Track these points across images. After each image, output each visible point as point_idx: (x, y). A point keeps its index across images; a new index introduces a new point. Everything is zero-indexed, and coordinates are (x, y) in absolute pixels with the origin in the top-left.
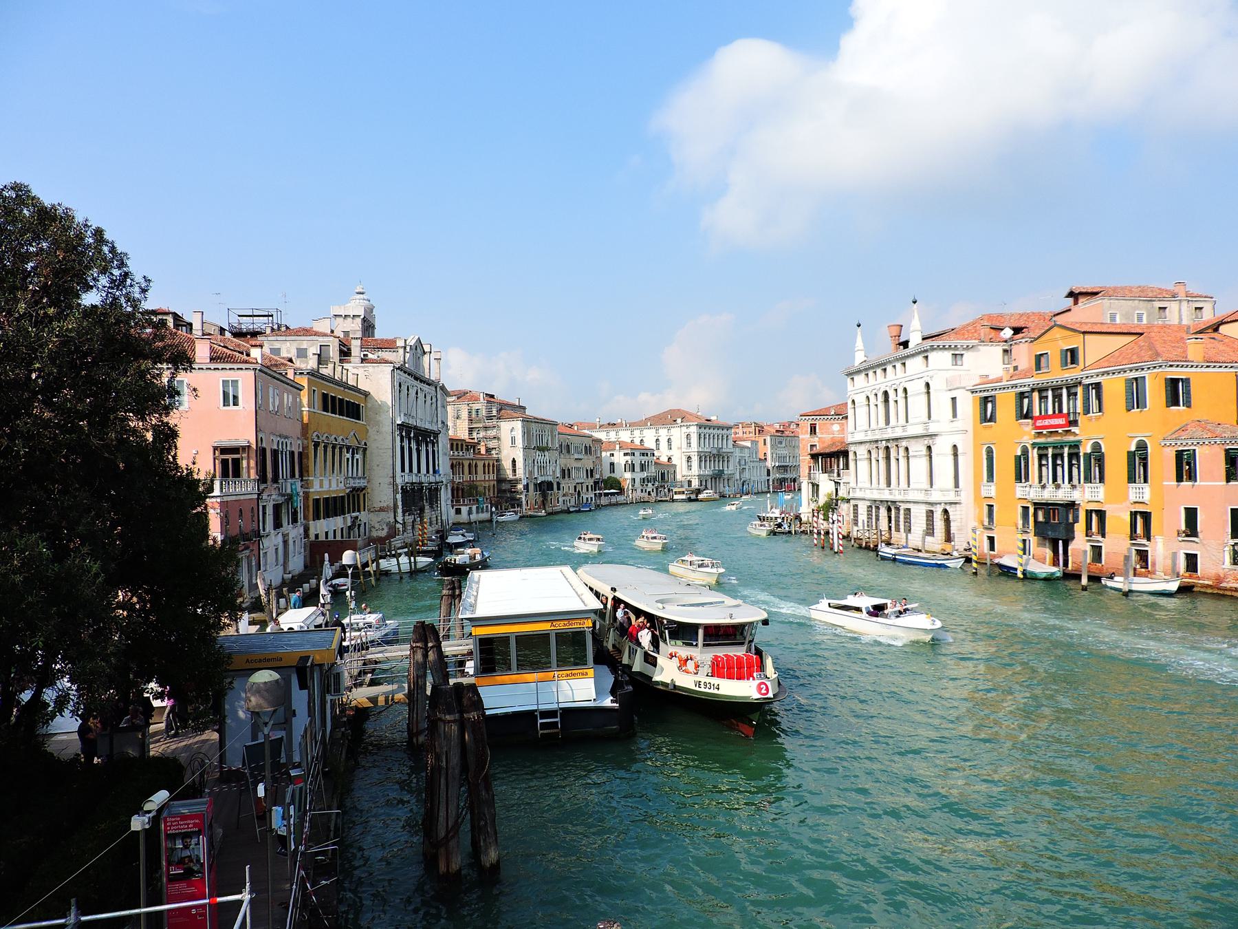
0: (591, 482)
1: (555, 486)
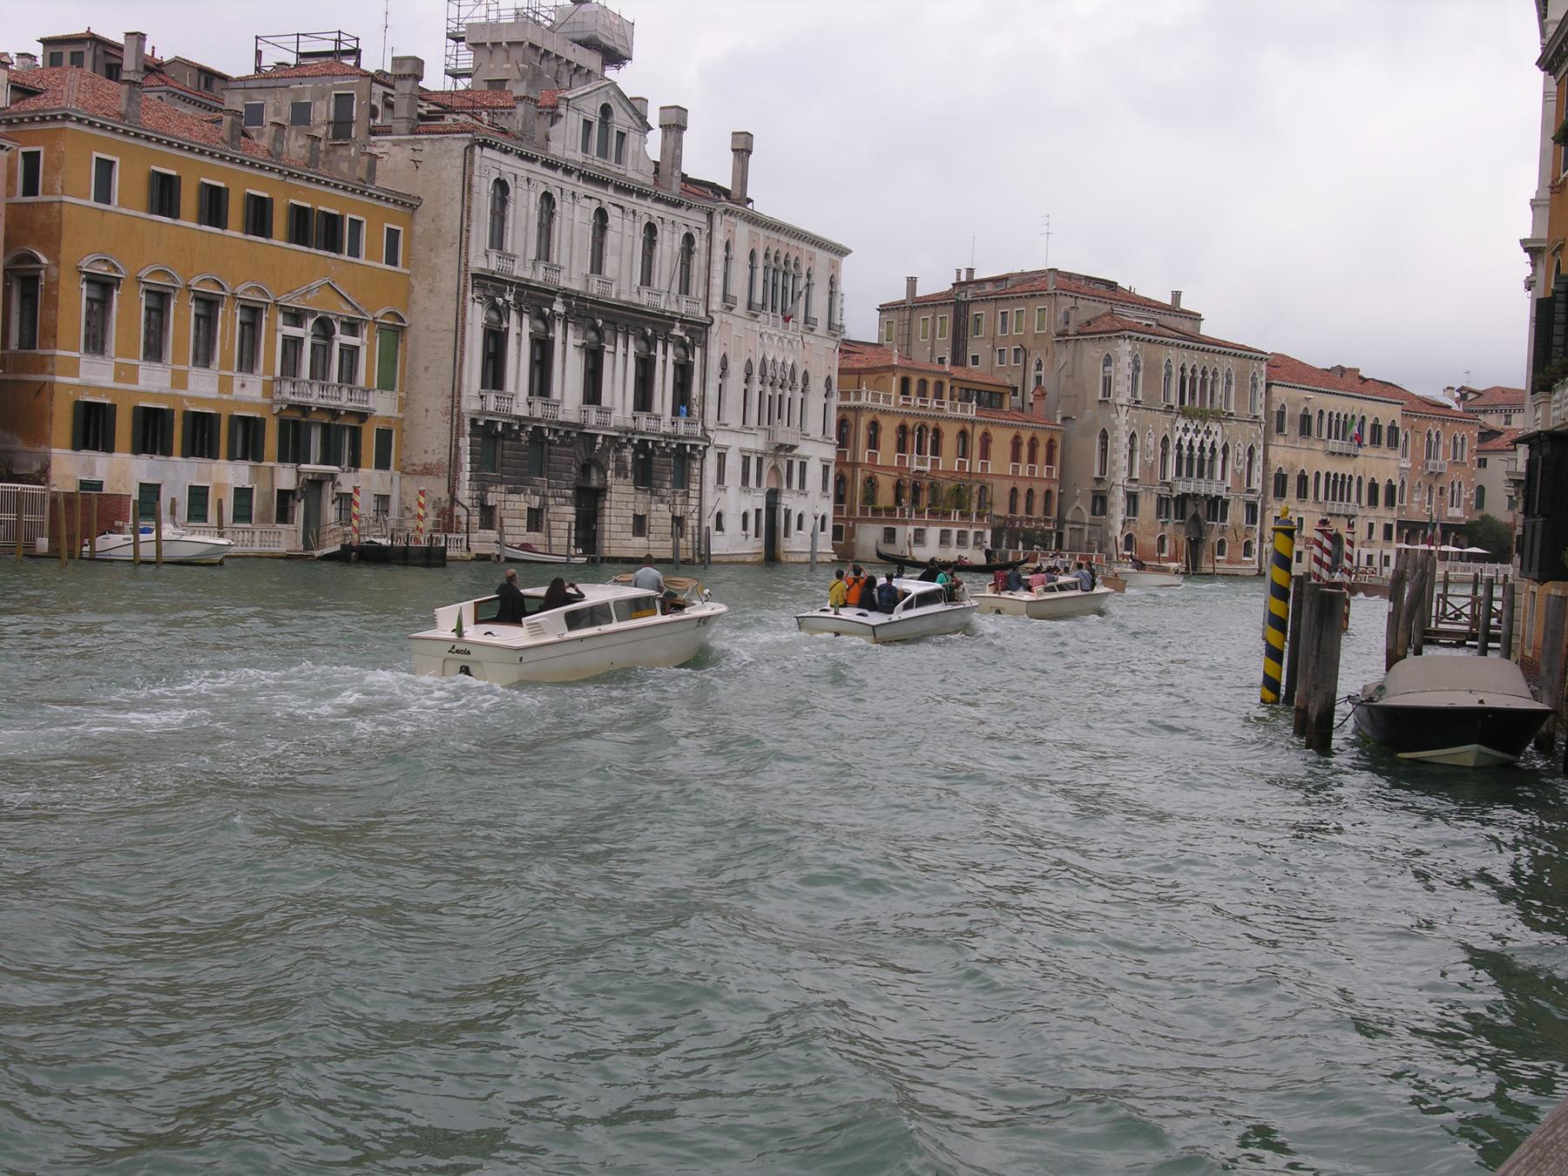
0: (1384, 515)
1: (1236, 513)
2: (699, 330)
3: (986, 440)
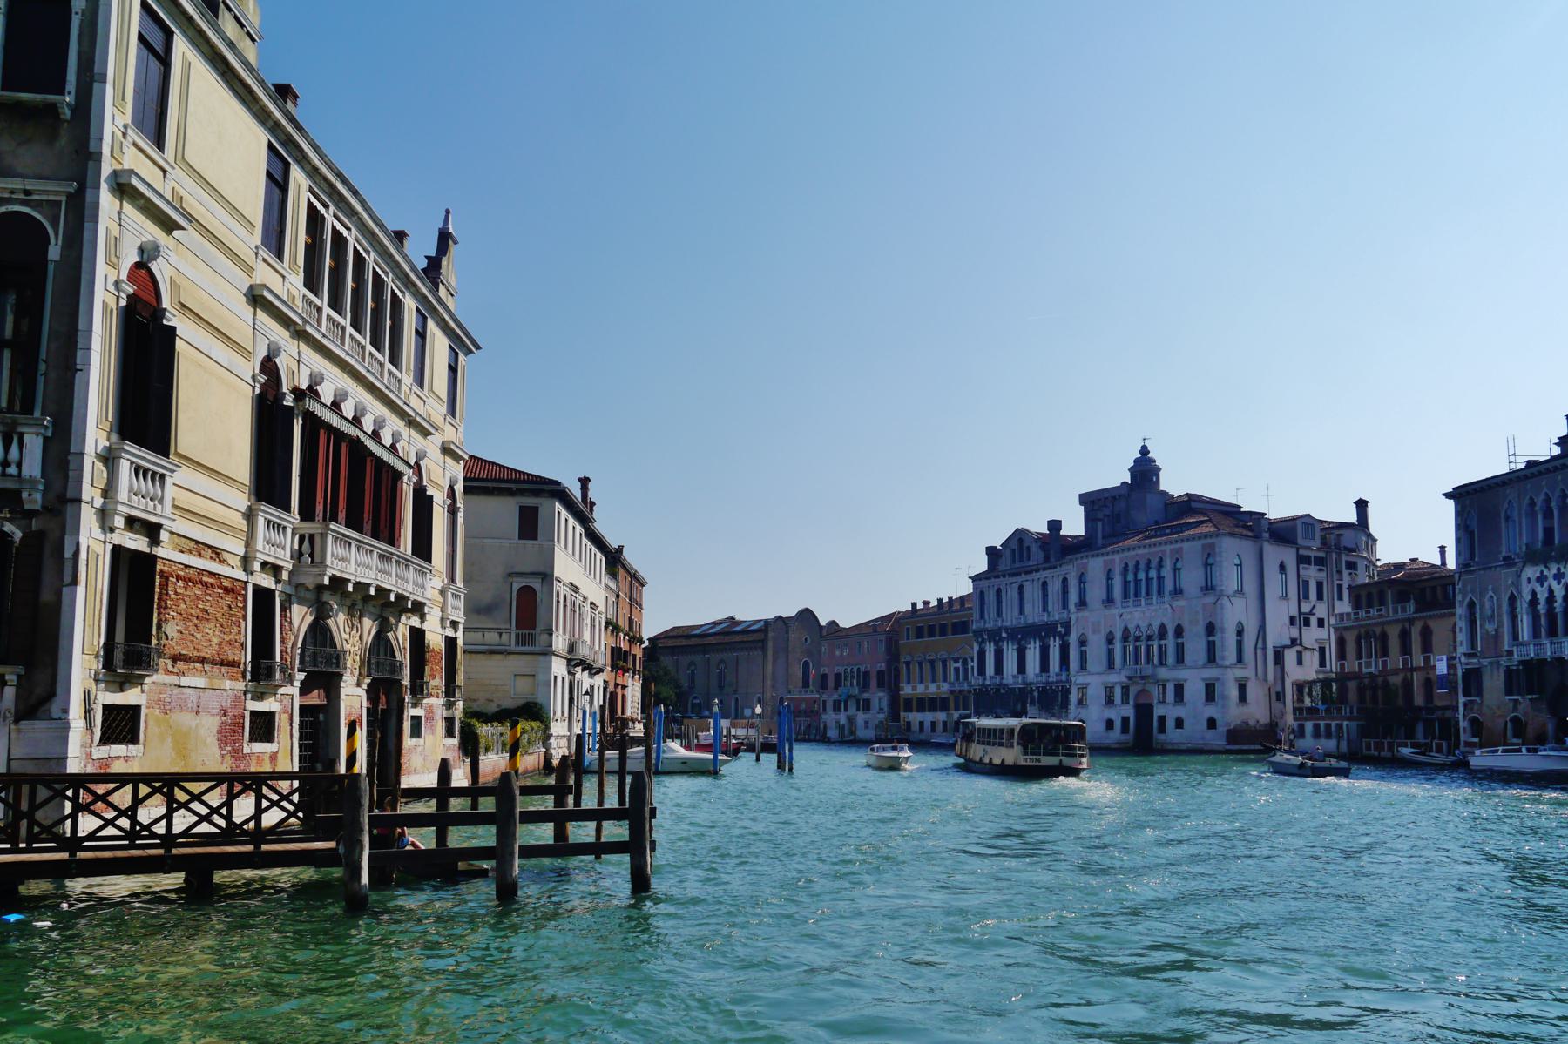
2: (1067, 625)
3: (1426, 634)
